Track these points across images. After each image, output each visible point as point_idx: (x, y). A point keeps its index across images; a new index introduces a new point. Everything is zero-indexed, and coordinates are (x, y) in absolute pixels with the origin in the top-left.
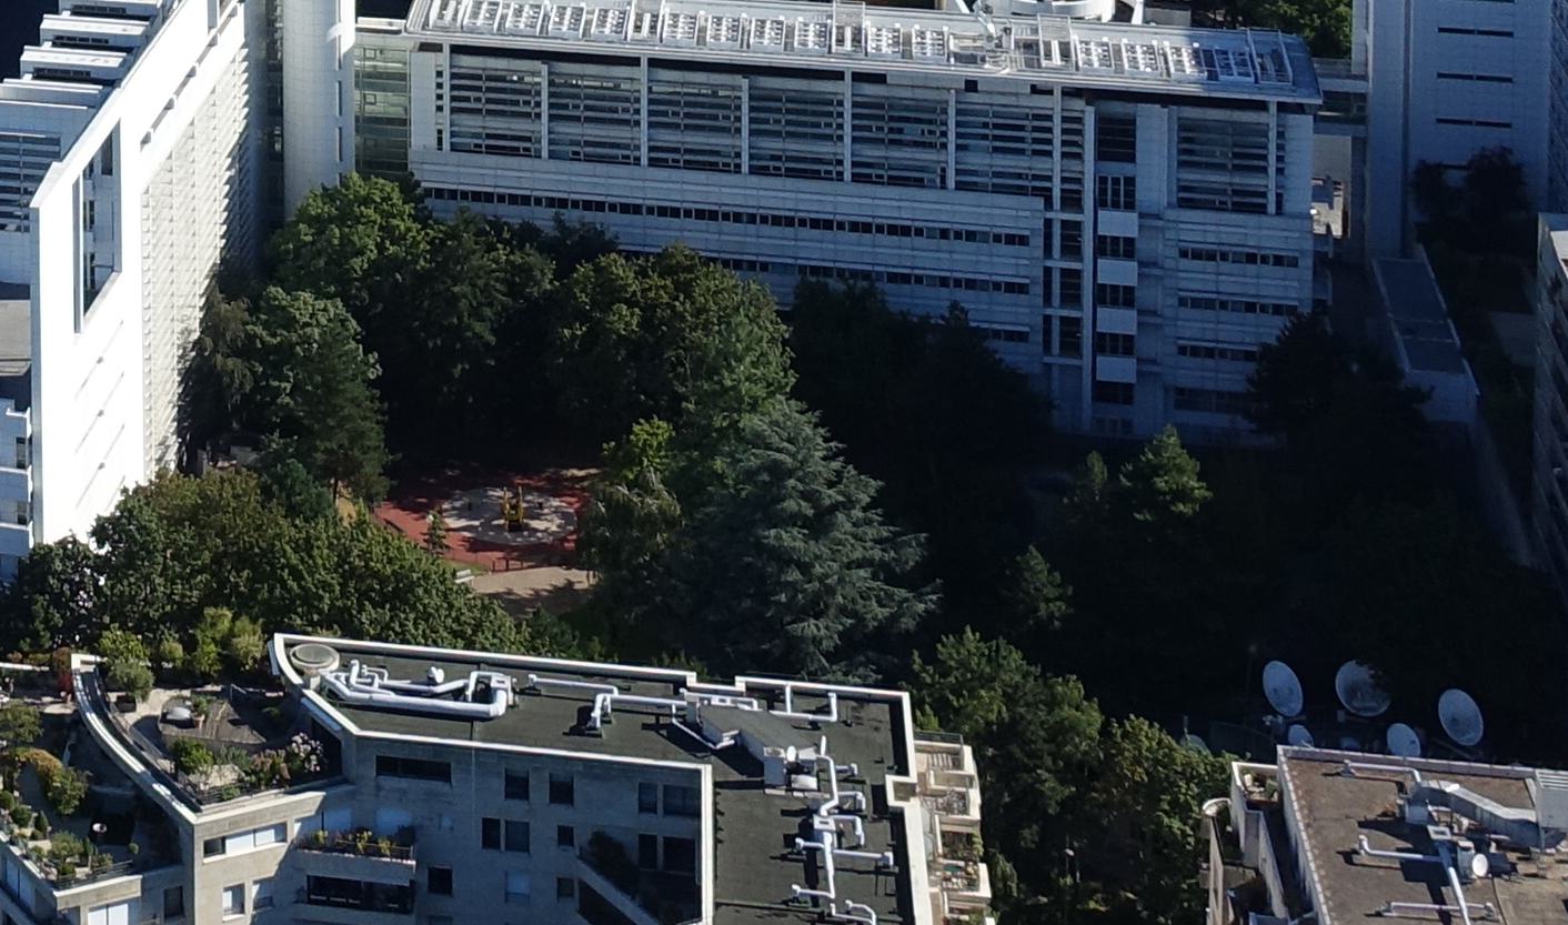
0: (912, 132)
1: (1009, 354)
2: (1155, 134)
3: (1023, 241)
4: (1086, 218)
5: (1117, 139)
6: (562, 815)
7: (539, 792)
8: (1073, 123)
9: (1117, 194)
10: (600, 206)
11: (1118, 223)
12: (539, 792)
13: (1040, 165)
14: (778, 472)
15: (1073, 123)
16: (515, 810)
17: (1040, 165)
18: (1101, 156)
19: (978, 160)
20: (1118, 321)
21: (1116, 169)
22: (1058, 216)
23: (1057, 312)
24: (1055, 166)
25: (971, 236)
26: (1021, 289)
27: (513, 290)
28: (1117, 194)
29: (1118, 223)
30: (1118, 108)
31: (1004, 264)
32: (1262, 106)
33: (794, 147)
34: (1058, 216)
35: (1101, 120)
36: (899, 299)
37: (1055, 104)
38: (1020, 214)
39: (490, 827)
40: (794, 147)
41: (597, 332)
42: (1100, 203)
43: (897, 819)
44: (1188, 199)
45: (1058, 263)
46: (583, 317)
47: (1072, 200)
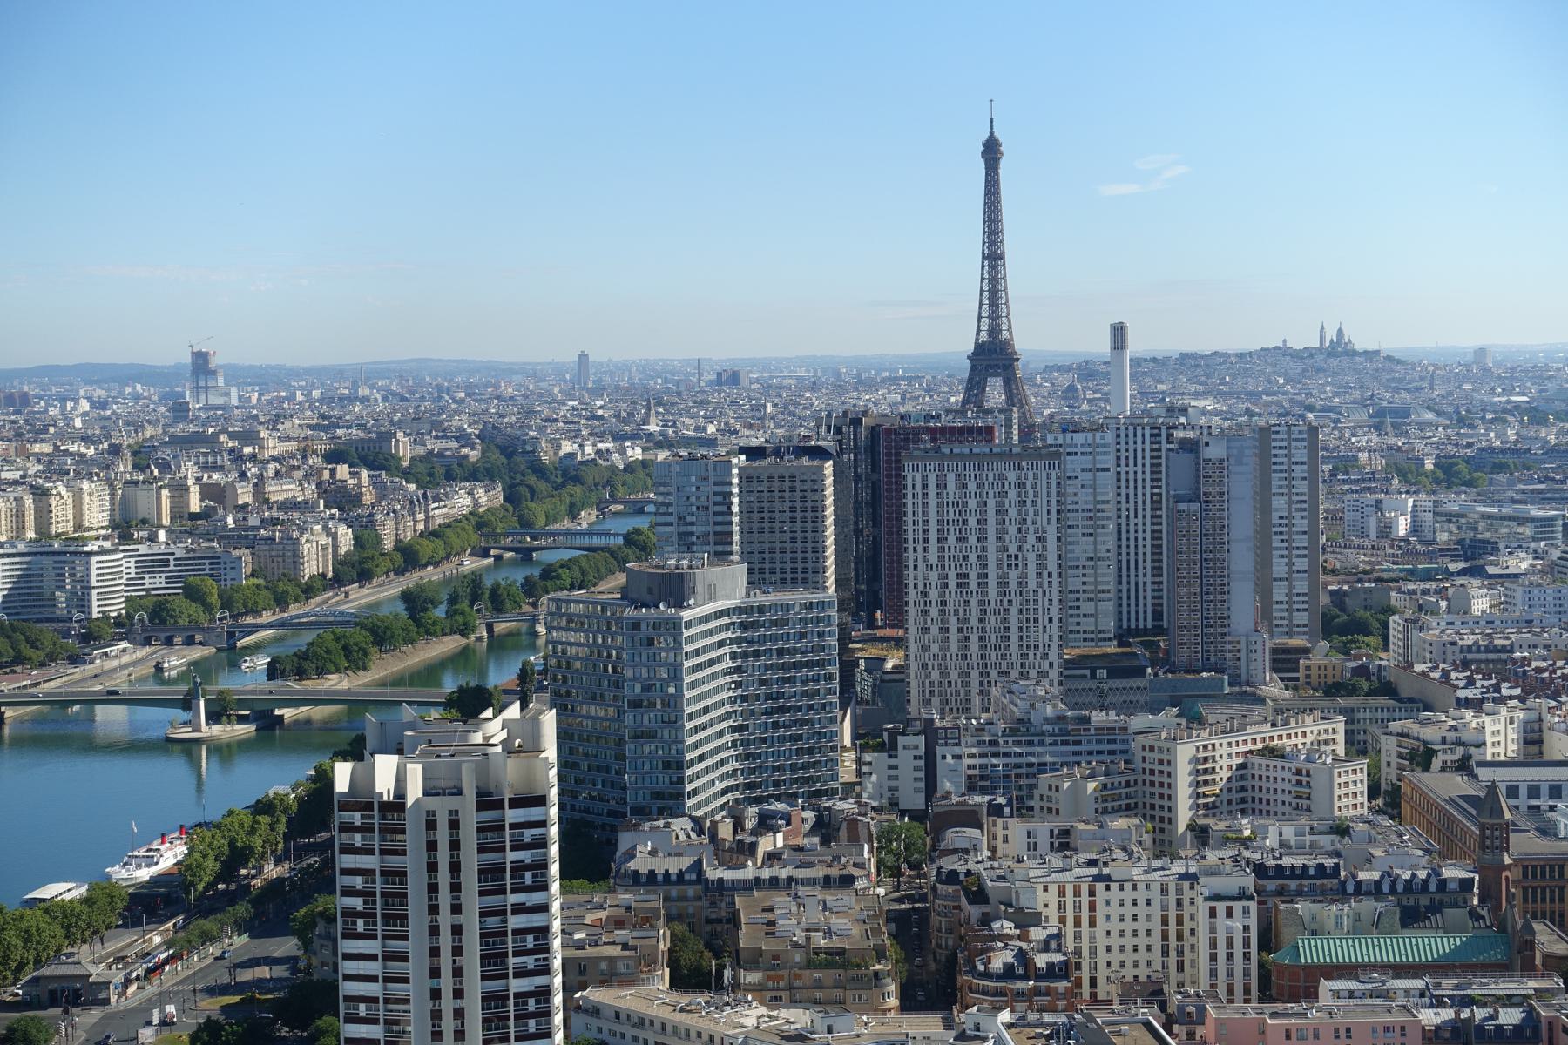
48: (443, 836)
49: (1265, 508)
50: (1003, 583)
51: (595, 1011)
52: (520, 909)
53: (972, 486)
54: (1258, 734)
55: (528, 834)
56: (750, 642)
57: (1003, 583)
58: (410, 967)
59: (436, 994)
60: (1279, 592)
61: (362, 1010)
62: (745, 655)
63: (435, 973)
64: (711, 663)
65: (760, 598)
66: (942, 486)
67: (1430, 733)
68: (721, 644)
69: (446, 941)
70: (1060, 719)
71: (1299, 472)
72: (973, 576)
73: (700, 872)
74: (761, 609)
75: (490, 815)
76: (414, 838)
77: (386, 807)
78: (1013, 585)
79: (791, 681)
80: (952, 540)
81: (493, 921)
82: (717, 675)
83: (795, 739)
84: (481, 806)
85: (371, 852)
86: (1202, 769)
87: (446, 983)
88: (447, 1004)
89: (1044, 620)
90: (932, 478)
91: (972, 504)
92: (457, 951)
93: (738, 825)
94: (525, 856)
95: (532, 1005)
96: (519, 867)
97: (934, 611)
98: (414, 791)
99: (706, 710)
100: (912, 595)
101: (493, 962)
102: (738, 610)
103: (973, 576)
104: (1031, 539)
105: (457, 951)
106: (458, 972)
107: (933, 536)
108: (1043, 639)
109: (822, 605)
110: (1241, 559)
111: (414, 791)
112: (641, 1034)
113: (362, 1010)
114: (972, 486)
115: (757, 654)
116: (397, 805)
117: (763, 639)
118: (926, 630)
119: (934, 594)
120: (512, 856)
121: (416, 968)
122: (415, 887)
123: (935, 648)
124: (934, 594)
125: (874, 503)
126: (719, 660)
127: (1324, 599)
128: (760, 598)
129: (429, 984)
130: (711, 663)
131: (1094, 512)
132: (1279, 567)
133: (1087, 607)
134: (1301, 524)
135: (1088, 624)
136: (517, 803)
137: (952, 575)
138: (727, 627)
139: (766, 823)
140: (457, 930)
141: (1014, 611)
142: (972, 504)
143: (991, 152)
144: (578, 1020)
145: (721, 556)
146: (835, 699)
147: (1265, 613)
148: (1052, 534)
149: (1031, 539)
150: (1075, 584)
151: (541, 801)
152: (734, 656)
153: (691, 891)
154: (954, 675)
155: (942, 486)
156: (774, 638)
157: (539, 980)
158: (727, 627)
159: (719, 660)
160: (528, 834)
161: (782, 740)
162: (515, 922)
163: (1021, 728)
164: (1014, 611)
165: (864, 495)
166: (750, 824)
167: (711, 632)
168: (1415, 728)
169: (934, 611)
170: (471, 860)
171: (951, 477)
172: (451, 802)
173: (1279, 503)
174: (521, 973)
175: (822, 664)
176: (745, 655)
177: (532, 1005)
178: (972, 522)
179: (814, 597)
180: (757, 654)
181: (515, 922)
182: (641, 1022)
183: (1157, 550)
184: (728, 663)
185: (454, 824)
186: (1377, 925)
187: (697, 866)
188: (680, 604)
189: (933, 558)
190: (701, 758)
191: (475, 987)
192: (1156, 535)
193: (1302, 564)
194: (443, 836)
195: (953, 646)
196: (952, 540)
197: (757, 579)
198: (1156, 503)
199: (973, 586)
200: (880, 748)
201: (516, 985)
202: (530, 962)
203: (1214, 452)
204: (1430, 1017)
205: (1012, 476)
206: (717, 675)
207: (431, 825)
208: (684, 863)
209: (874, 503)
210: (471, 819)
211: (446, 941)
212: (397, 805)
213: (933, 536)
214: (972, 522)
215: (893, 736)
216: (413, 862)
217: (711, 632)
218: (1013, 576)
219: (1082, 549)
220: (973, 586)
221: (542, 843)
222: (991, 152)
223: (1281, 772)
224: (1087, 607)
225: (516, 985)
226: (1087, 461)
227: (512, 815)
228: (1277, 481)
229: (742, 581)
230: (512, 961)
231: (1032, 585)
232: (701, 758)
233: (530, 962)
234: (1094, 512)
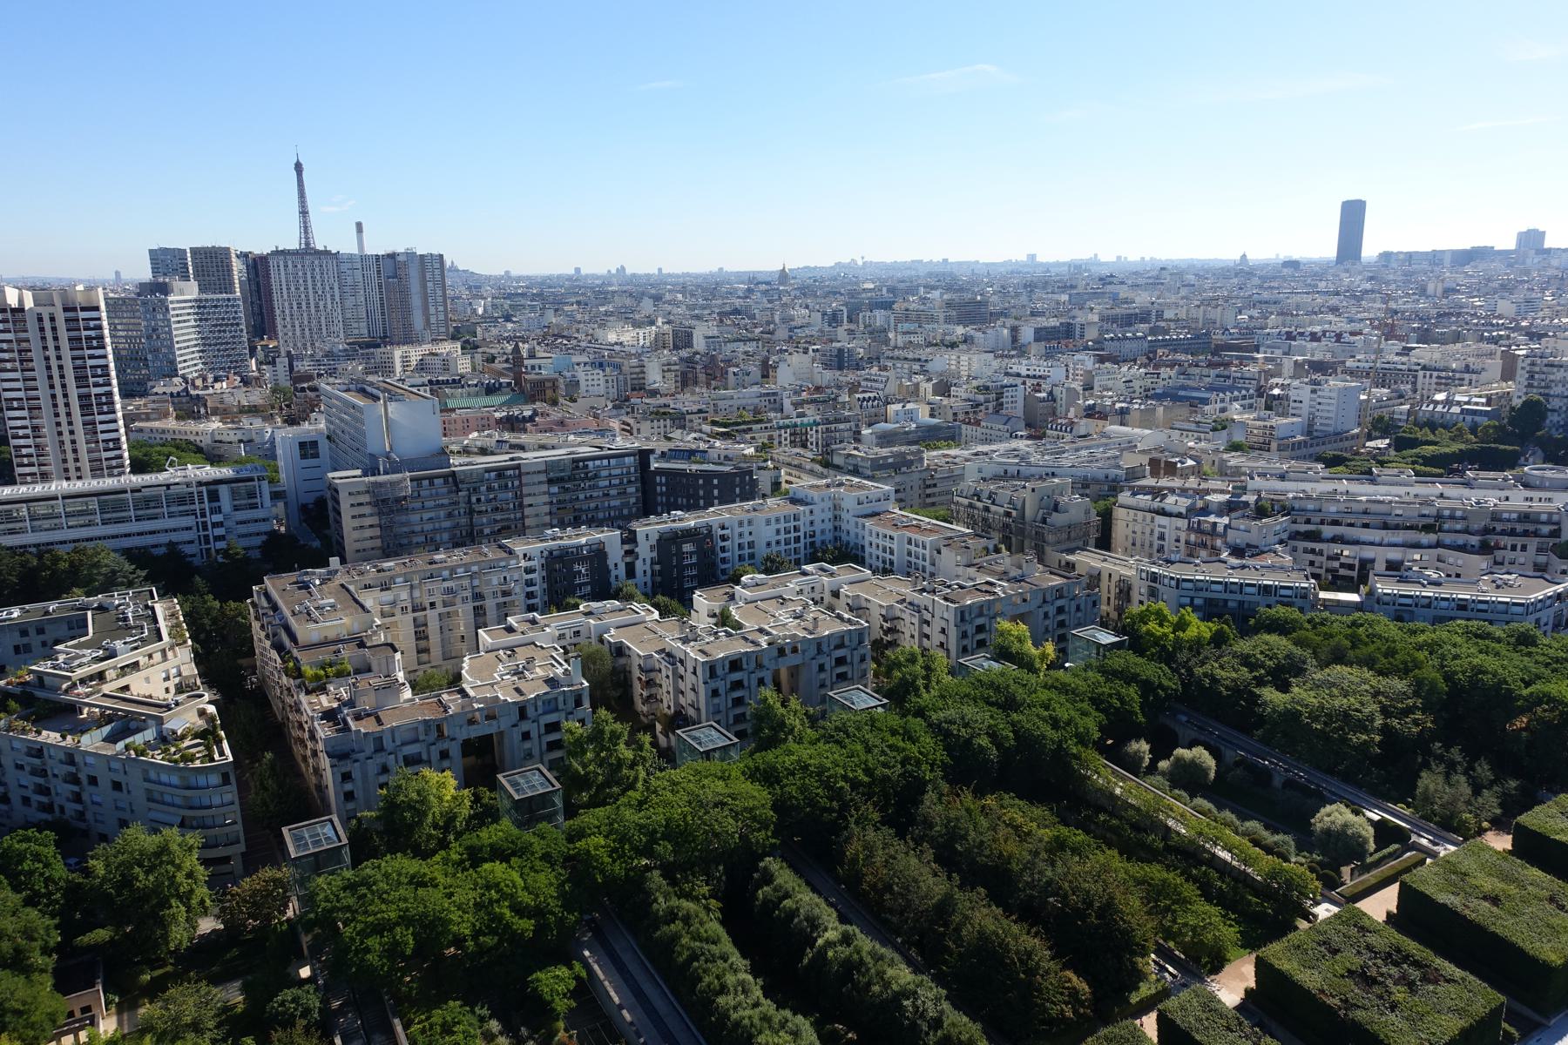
0: (152, 504)
1: (188, 549)
2: (224, 491)
3: (190, 528)
4: (208, 519)
5: (214, 496)
6: (42, 638)
7: (32, 632)
8: (200, 493)
9: (219, 510)
10: (52, 544)
11: (217, 518)
12: (32, 632)
13: (192, 507)
14: (114, 572)
15: (200, 493)
16: (25, 640)
17: (192, 507)
18: (210, 501)
19: (173, 509)
20: (219, 531)
21: (216, 504)
22: (200, 520)
23: (202, 533)
24: (197, 506)
25: (175, 530)
26: (190, 528)
27: (22, 566)
28: (213, 511)
29: (217, 518)
30: (212, 487)
31: (187, 536)
32: (251, 479)
33: (114, 515)
34: (200, 520)
35: (208, 491)
36: (155, 551)
37: (194, 489)
38: (189, 521)
39: (17, 649)
40: (114, 515)
41: (54, 572)
42: (211, 513)
43: (153, 609)
44: (236, 508)
45: (202, 533)
46: (49, 568)
47: (203, 515)
48: (47, 324)
49: (424, 287)
50: (317, 307)
51: (141, 430)
52: (92, 357)
53: (299, 266)
54: (426, 348)
55: (92, 324)
56: (203, 314)
57: (317, 307)
58: (38, 383)
59: (47, 359)
60: (433, 320)
61: (15, 404)
62: (201, 320)
63: (52, 387)
64: (185, 321)
65: (204, 296)
66: (286, 266)
67: (493, 351)
68: (189, 314)
69: (55, 372)
70: (346, 350)
71: (437, 272)
72: (304, 304)
73: (188, 392)
74: (206, 300)
75: (71, 314)
76: (32, 325)
77: (14, 310)
78: (321, 308)
79: (224, 331)
80: (293, 289)
81: (79, 362)
82: (187, 327)
83: (229, 356)
84: (66, 310)
85: (16, 371)
86: (405, 361)
87: (63, 419)
88: (60, 400)
89: (336, 322)
90: (281, 263)
91: (300, 274)
92: (62, 377)
93: (205, 379)
94: (92, 333)
95: (104, 399)
96: (89, 338)
97: (288, 319)
98: (29, 303)
99: (185, 341)
100: (278, 312)
101: (81, 380)
102: (196, 300)
103: (304, 304)
104: (327, 288)
105: (62, 377)
106: (64, 386)
107: (284, 287)
108: (336, 329)
109: (235, 299)
110: (416, 301)
111: (29, 303)
112: (164, 436)
113: (15, 404)
114: (299, 266)
115: (206, 320)
116: (21, 310)
117: (209, 313)
118: (285, 327)
119: (287, 312)
120: (84, 333)
121: (42, 382)
122: (35, 345)
123: (290, 334)
124: (287, 312)
125: (258, 291)
126: (188, 321)
127: (451, 330)
128: (204, 296)
129: (49, 392)
130: (185, 321)
131: (354, 286)
132: (432, 310)
133: (355, 325)
134: (439, 293)
135: (356, 332)
136: (83, 309)
137: (295, 303)
138: (191, 307)
139: (217, 379)
140: (61, 367)
141: (323, 318)
142: (300, 274)
143: (299, 168)
144: (132, 436)
145: (186, 278)
146: (247, 351)
147: (428, 323)
148: (336, 286)
149: (327, 288)
150: (349, 316)
151: (97, 309)
152: (195, 320)
153: (184, 400)
154: (299, 345)
155: (286, 266)
156: (214, 313)
157: (107, 389)
158: (191, 307)
159: (188, 321)
160: (92, 324)
161: (223, 356)
162: (90, 362)
163: (329, 355)
164: (323, 318)
165: (253, 287)
166: (210, 380)
167: (184, 308)
168: (488, 350)
169: (288, 319)
170: (64, 335)
171: (290, 263)
172: (51, 309)
173: (430, 285)
174: (97, 385)
175: (237, 324)
176: (201, 320)
177: (104, 399)
178: (301, 281)
179: (231, 296)
180: (206, 320)
181: (90, 362)
182: (163, 432)
183: (382, 305)
184: (192, 323)
185: (52, 319)
186: (477, 395)
187: (186, 390)
188: (166, 295)
189: (285, 297)
190: (185, 361)
191: (74, 393)
192: (381, 299)
193: (441, 308)
194: (47, 324)
195: (298, 333)
196: (293, 289)
197: (201, 290)
198: (380, 286)
199: (304, 308)
200: (269, 363)
201: (95, 391)
202: (101, 380)
203: (400, 259)
204: (497, 415)
205: (316, 262)
206: (187, 327)
207: (40, 319)
208: (180, 389)
209: (258, 291)
210: (61, 317)
211: (55, 372)
212: (21, 310)
213: (284, 287)
214: (301, 281)
215: (274, 358)
216: (32, 333)
217: (184, 308)
218: (321, 303)
219: (349, 302)
220: (304, 308)
221: (100, 328)
222: (299, 168)
223: (437, 361)
224: (355, 325)
225: (95, 391)
226: (350, 266)
227: (82, 315)
228: (428, 276)
229: (196, 289)
230: (91, 380)
231: (330, 307)
232: (185, 361)
233: (101, 380)
234: (354, 286)
